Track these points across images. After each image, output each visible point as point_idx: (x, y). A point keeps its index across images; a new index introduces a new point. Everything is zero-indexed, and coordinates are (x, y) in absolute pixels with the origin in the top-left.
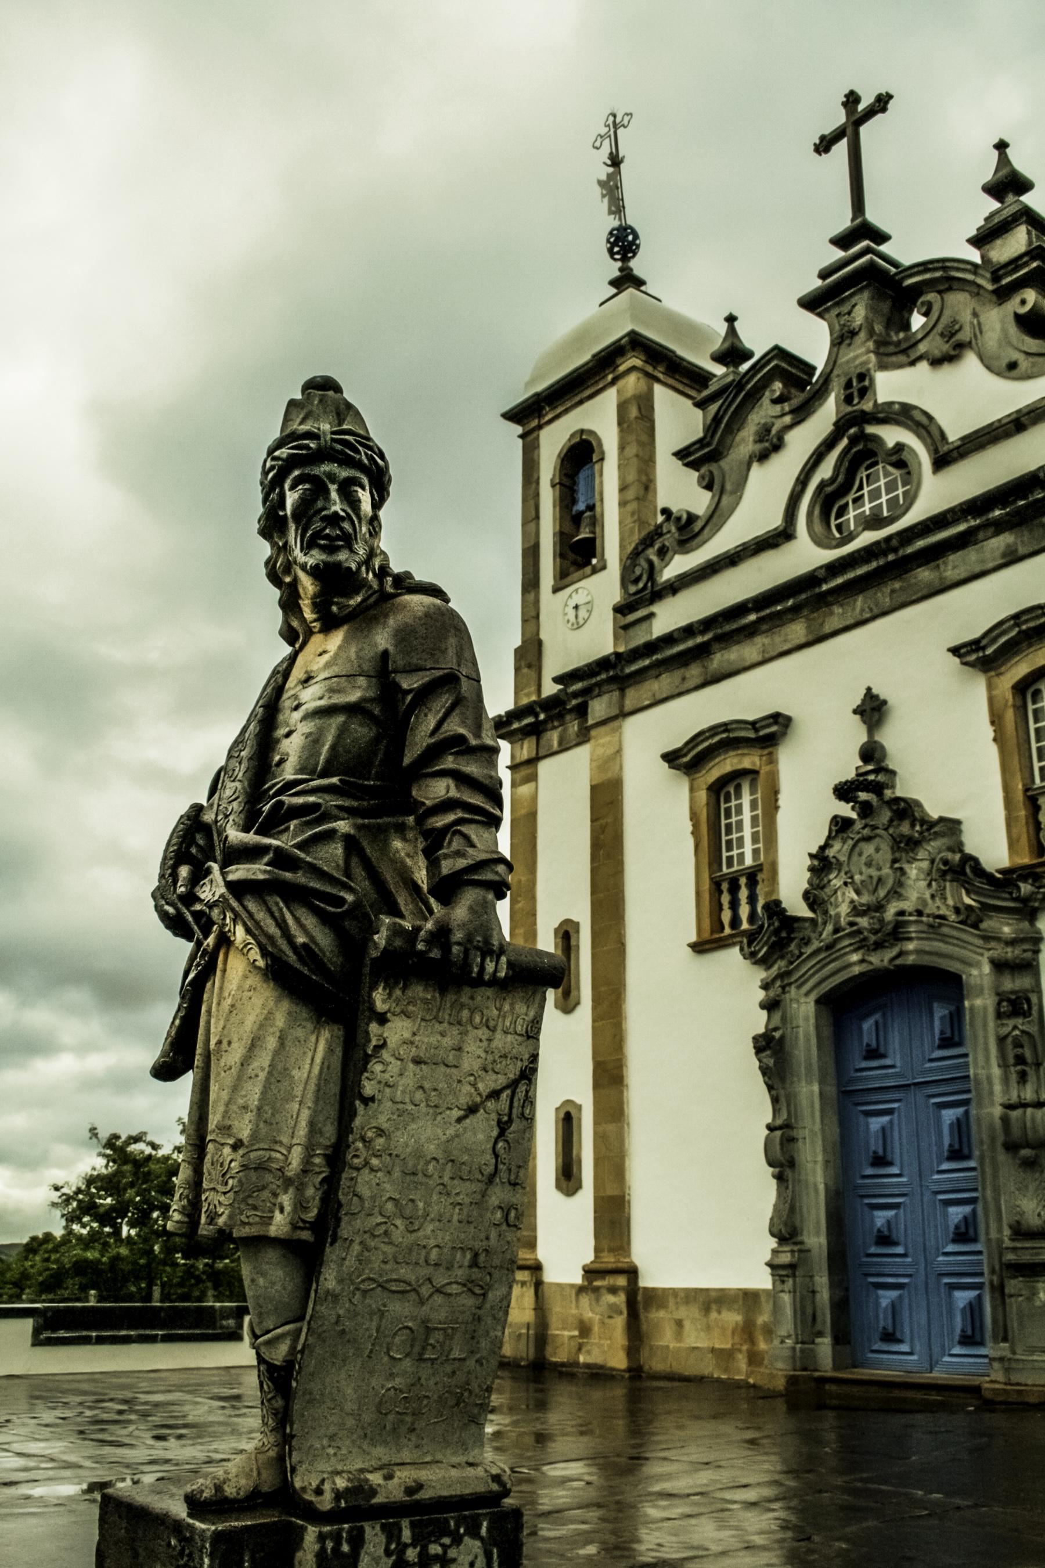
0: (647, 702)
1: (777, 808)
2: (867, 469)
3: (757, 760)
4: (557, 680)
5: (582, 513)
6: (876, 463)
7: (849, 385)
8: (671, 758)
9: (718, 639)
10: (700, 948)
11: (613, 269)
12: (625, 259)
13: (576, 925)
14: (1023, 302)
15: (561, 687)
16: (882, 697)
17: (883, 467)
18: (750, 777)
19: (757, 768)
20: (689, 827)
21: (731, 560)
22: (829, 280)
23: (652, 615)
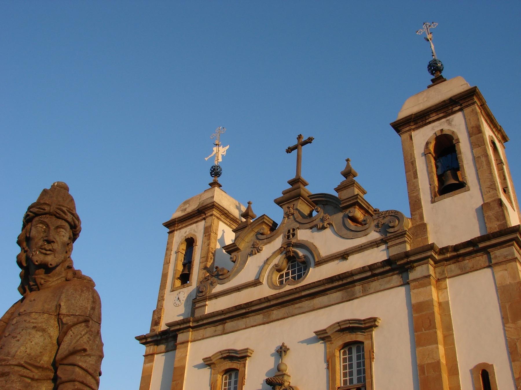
0: (200, 338)
2: (291, 263)
7: (289, 231)
11: (211, 180)
15: (168, 327)
16: (288, 347)
19: (238, 369)
22: (285, 195)
23: (206, 305)
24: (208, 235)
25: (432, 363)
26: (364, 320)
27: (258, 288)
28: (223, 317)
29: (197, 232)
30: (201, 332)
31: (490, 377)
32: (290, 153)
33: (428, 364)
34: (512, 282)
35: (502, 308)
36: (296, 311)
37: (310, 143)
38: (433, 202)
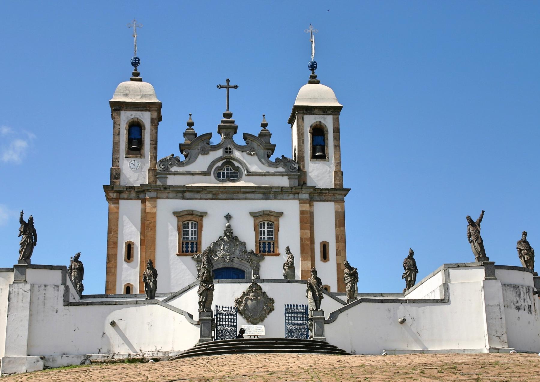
1: (202, 230)
2: (226, 167)
3: (197, 219)
4: (140, 185)
5: (132, 139)
6: (229, 167)
7: (227, 149)
8: (174, 213)
9: (188, 191)
10: (178, 255)
12: (136, 66)
13: (133, 244)
14: (270, 153)
15: (140, 185)
17: (230, 169)
18: (191, 222)
20: (177, 229)
21: (193, 174)
23: (167, 178)
24: (154, 125)
25: (306, 238)
26: (277, 213)
27: (207, 177)
28: (185, 189)
29: (143, 119)
30: (164, 195)
31: (327, 247)
32: (219, 88)
33: (304, 238)
34: (341, 211)
35: (336, 221)
36: (234, 197)
37: (236, 89)
38: (310, 161)
